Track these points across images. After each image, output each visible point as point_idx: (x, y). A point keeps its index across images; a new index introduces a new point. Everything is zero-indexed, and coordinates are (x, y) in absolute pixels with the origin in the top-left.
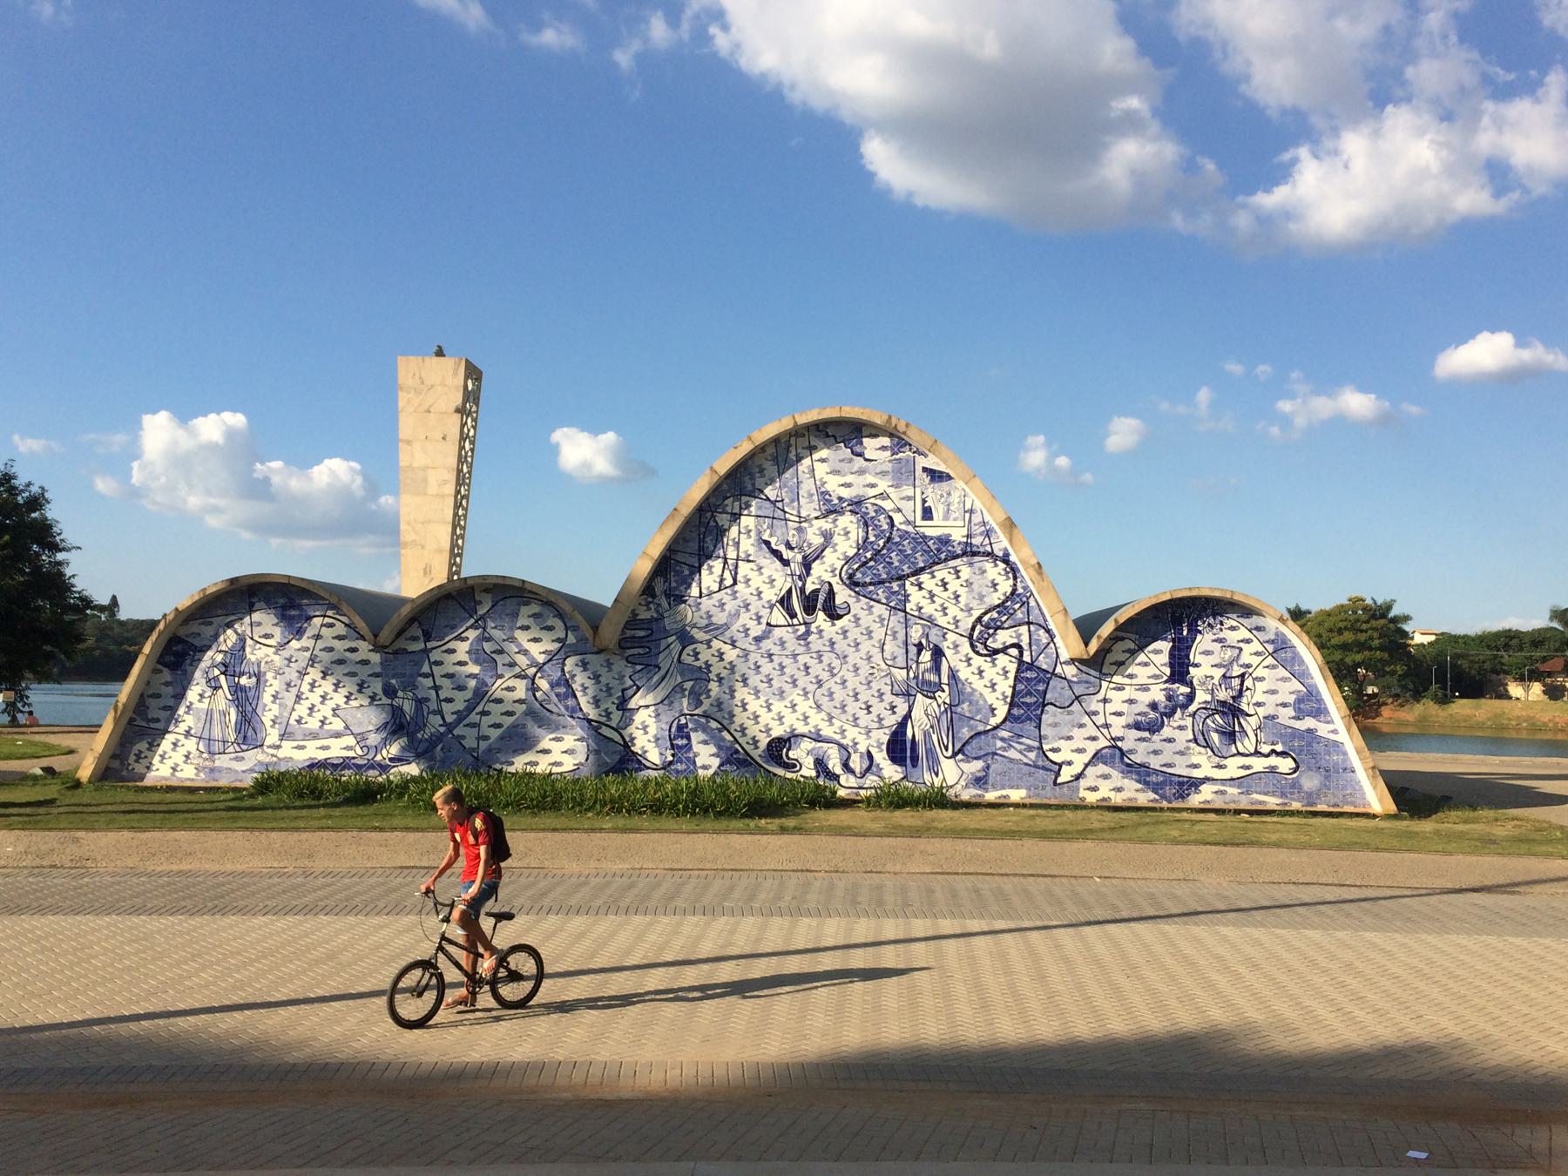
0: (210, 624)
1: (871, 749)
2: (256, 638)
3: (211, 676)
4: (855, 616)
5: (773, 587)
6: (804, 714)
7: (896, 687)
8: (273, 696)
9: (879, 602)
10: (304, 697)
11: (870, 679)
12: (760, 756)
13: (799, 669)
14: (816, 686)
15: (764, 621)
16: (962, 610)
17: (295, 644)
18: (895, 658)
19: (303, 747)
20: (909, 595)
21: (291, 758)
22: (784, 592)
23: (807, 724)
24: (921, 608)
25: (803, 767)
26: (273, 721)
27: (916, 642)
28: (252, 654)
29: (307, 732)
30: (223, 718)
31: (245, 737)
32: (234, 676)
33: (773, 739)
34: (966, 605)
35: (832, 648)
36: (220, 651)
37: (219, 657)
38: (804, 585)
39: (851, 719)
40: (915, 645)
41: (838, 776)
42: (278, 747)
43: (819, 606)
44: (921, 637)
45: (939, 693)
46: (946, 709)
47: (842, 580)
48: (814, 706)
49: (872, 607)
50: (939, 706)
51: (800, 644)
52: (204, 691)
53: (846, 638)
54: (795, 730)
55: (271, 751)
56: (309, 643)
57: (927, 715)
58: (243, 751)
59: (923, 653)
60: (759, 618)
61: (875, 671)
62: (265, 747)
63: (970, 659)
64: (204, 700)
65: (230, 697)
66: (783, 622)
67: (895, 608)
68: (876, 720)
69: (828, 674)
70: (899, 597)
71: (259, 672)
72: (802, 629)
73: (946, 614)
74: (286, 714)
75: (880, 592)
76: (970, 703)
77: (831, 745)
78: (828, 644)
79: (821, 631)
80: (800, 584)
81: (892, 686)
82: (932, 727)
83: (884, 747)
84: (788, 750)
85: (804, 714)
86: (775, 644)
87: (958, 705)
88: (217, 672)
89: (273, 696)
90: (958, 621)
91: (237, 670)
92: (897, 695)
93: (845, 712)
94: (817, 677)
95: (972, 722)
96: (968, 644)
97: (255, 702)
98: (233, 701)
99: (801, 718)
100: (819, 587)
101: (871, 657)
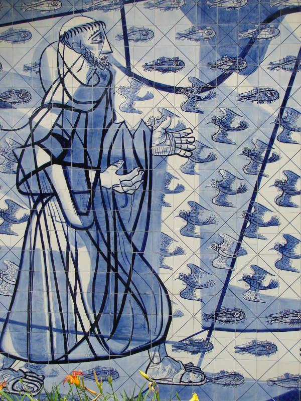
0: (25, 37)
2: (138, 69)
3: (28, 167)
8: (185, 216)
10: (266, 218)
17: (237, 83)
19: (268, 349)
21: (238, 376)
26: (185, 278)
28: (130, 109)
29: (277, 309)
30: (60, 272)
31: (117, 320)
32: (86, 166)
36: (50, 106)
37: (48, 121)
42: (204, 347)
52: (12, 205)
55: (185, 357)
56: (278, 80)
58: (113, 356)
62: (169, 347)
64: (14, 227)
65: (76, 219)
71: (149, 155)
74: (221, 263)
88: (43, 158)
89: (185, 216)
91: (94, 151)
97: (140, 232)
98: (86, 229)
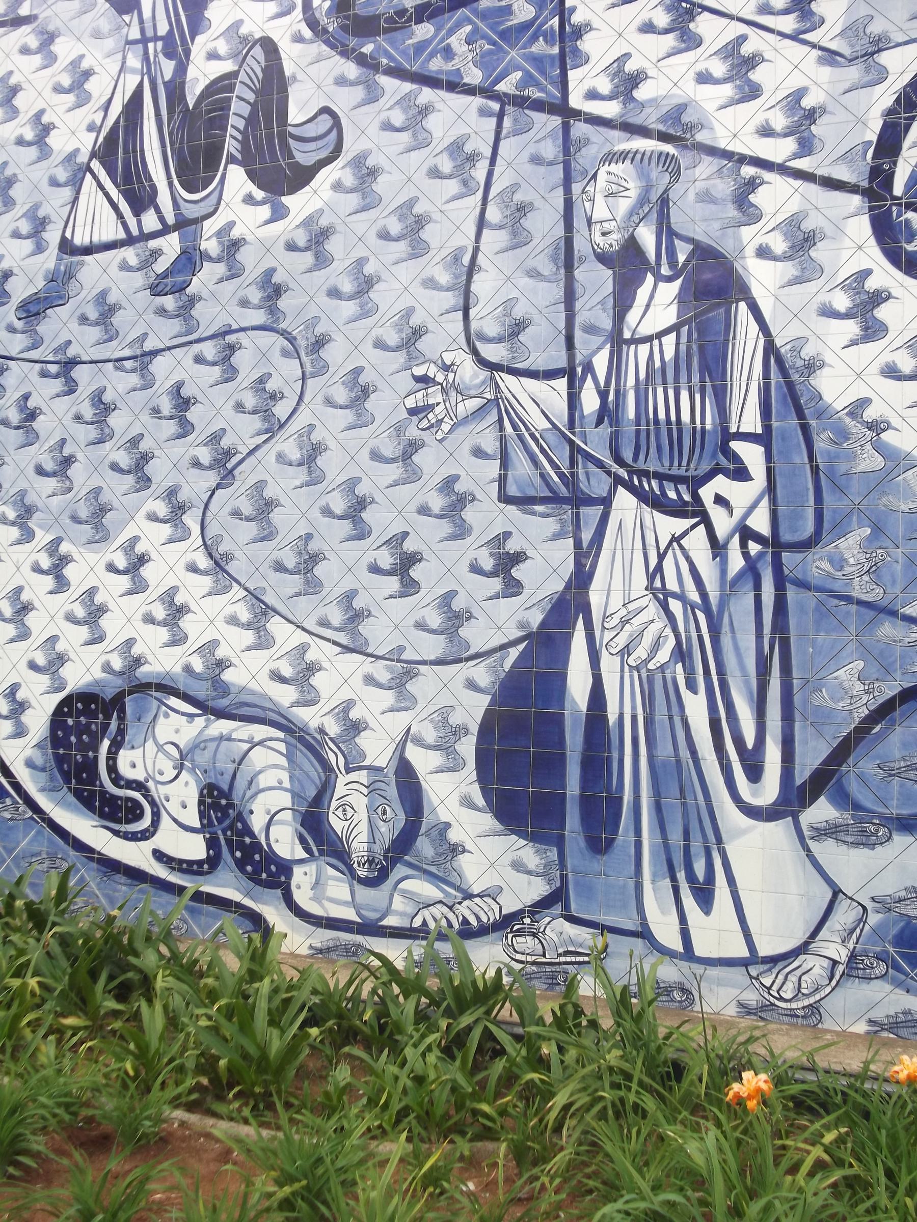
1: (413, 754)
4: (358, 162)
5: (83, 100)
6: (169, 597)
7: (522, 467)
9: (453, 85)
11: (413, 432)
12: (30, 764)
13: (156, 411)
14: (211, 478)
15: (52, 236)
16: (830, 56)
18: (518, 328)
20: (579, 32)
22: (116, 109)
23: (178, 639)
24: (635, 80)
25: (165, 820)
27: (614, 241)
33: (67, 701)
34: (851, 31)
35: (273, 311)
38: (181, 69)
39: (337, 617)
40: (603, 258)
41: (285, 868)
43: (231, 146)
44: (636, 214)
45: (720, 484)
46: (752, 569)
47: (312, 24)
48: (203, 562)
49: (425, 111)
50: (717, 547)
51: (162, 312)
53: (322, 261)
54: (138, 661)
57: (662, 597)
59: (642, 294)
60: (40, 225)
61: (435, 396)
63: (879, 298)
66: (110, 230)
67: (520, 102)
68: (435, 620)
69: (256, 423)
70: (539, 47)
72: (171, 245)
73: (752, 92)
75: (457, 42)
76: (878, 530)
77: (260, 731)
78: (255, 296)
79: (236, 245)
80: (168, 68)
81: (505, 460)
82: (681, 654)
83: (467, 748)
84: (117, 745)
85: (169, 597)
86: (83, 319)
87: (805, 545)
90: (811, 115)
92: (524, 502)
93: (312, 586)
94: (215, 438)
95: (888, 629)
96: (861, 228)
99: (160, 612)
100: (228, 66)
101: (417, 333)
